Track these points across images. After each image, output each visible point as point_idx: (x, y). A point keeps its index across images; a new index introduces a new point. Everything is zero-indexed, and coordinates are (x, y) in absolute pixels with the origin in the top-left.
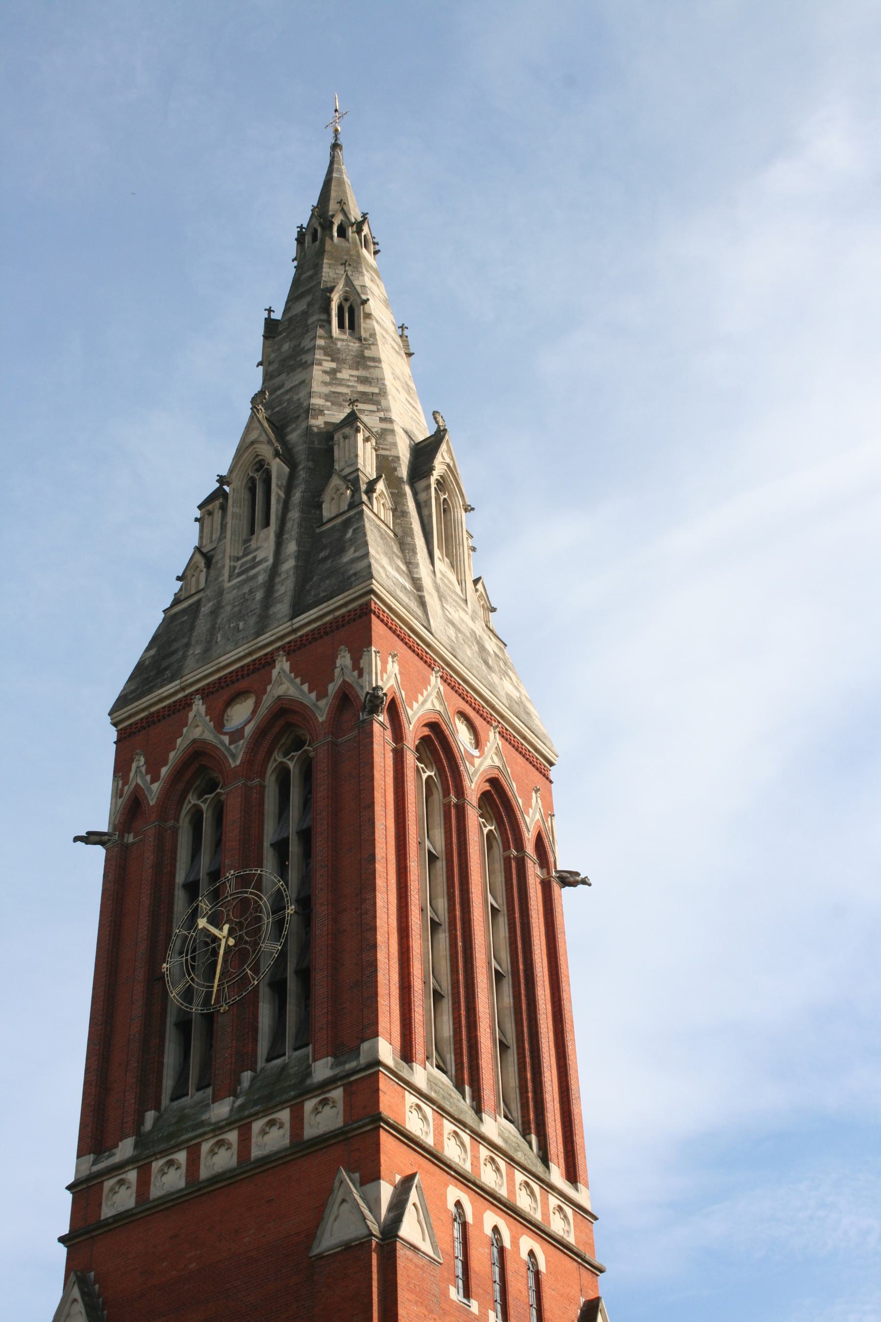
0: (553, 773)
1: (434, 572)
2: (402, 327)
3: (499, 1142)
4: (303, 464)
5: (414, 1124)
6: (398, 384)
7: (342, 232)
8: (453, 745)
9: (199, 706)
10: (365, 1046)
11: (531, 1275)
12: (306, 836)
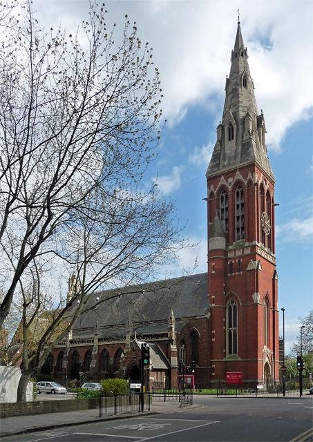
5: (259, 252)
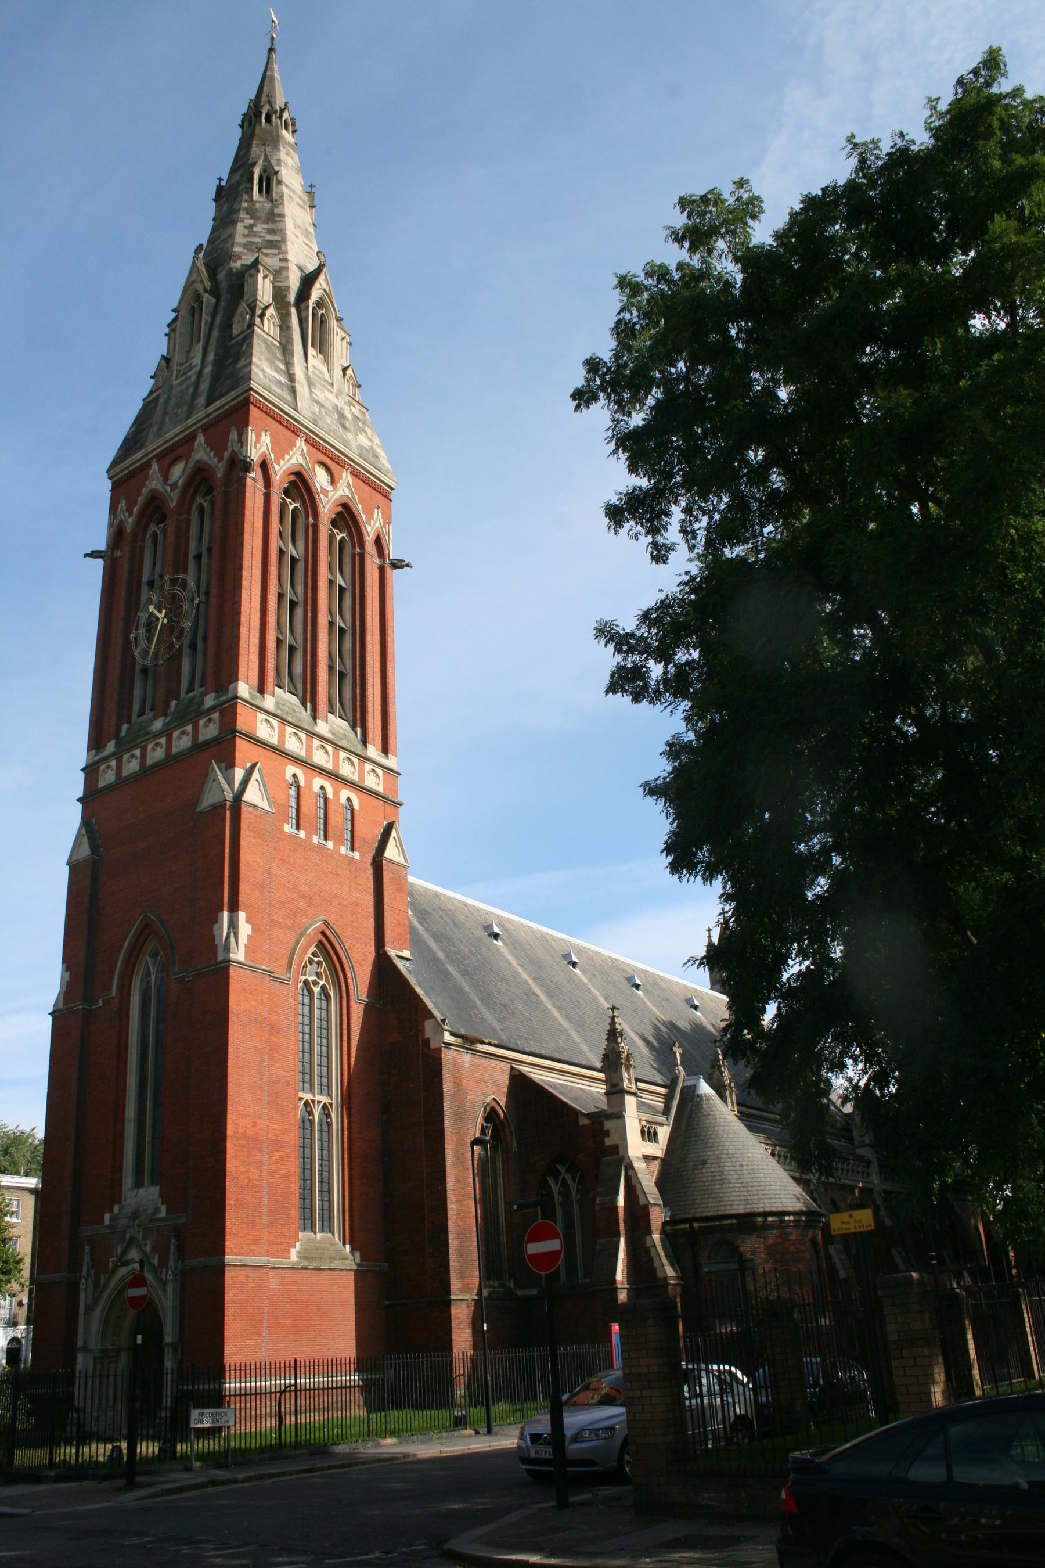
0: (393, 495)
1: (307, 368)
2: (311, 186)
3: (329, 736)
4: (224, 296)
6: (298, 232)
7: (268, 119)
8: (311, 485)
9: (155, 467)
10: (232, 686)
11: (349, 812)
12: (210, 550)
